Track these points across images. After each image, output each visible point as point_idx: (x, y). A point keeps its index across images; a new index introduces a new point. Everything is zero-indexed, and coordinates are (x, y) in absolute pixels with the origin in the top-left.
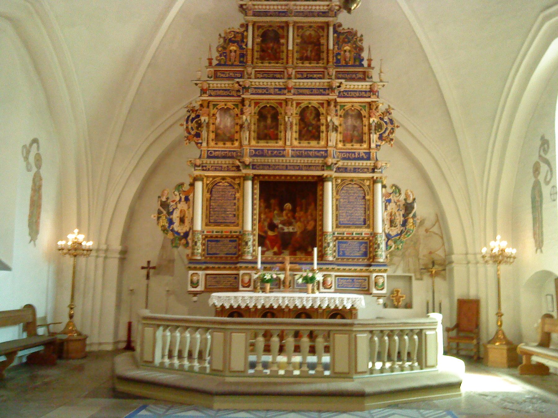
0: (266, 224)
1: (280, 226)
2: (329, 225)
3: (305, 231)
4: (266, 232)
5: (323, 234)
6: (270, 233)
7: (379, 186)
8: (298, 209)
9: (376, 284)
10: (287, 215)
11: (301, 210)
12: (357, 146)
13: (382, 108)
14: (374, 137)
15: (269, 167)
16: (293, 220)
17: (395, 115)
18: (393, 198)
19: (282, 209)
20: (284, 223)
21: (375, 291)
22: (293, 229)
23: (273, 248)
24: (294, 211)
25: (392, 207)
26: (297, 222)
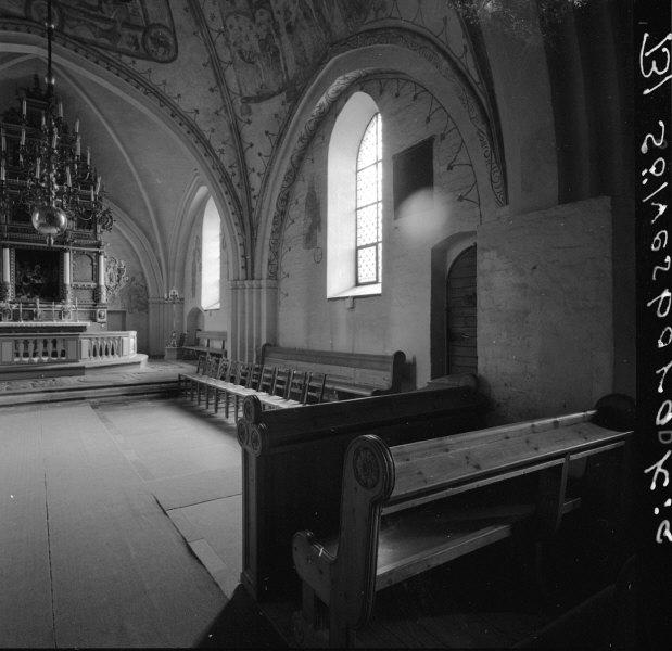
5: (65, 285)
7: (102, 257)
9: (100, 316)
12: (87, 231)
13: (104, 209)
14: (99, 226)
15: (25, 240)
17: (112, 214)
18: (112, 265)
20: (35, 277)
21: (99, 320)
25: (110, 270)
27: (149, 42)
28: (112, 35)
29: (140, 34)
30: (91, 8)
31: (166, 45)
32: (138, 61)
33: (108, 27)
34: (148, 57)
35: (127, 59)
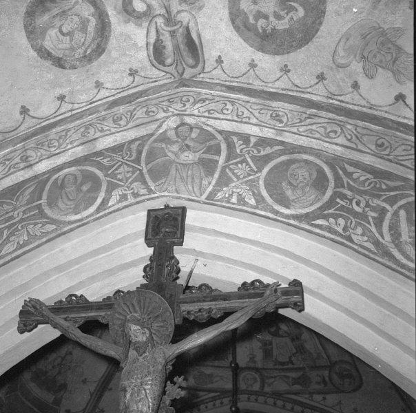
27: (335, 377)
28: (303, 380)
29: (326, 373)
30: (283, 364)
31: (350, 376)
32: (328, 396)
33: (300, 374)
34: (338, 390)
35: (318, 398)
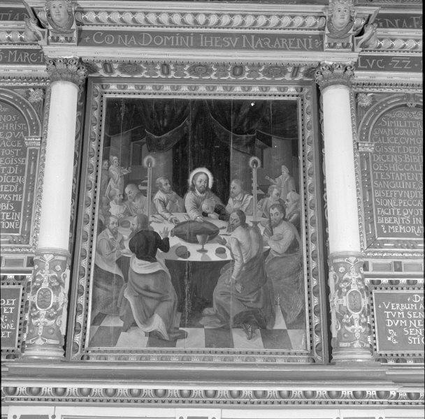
0: (126, 234)
1: (174, 242)
2: (346, 234)
3: (258, 264)
4: (123, 263)
6: (139, 266)
8: (235, 185)
10: (197, 206)
11: (247, 189)
16: (220, 224)
19: (180, 185)
22: (220, 252)
23: (147, 319)
24: (221, 190)
26: (231, 228)
